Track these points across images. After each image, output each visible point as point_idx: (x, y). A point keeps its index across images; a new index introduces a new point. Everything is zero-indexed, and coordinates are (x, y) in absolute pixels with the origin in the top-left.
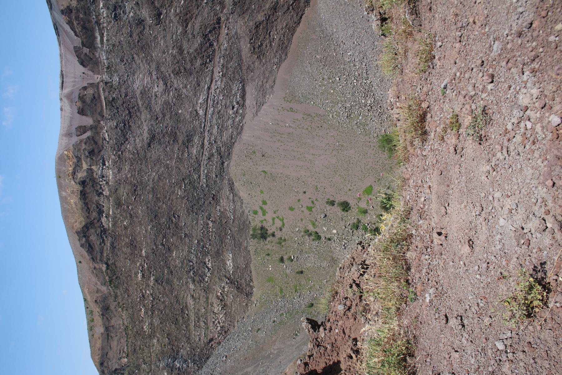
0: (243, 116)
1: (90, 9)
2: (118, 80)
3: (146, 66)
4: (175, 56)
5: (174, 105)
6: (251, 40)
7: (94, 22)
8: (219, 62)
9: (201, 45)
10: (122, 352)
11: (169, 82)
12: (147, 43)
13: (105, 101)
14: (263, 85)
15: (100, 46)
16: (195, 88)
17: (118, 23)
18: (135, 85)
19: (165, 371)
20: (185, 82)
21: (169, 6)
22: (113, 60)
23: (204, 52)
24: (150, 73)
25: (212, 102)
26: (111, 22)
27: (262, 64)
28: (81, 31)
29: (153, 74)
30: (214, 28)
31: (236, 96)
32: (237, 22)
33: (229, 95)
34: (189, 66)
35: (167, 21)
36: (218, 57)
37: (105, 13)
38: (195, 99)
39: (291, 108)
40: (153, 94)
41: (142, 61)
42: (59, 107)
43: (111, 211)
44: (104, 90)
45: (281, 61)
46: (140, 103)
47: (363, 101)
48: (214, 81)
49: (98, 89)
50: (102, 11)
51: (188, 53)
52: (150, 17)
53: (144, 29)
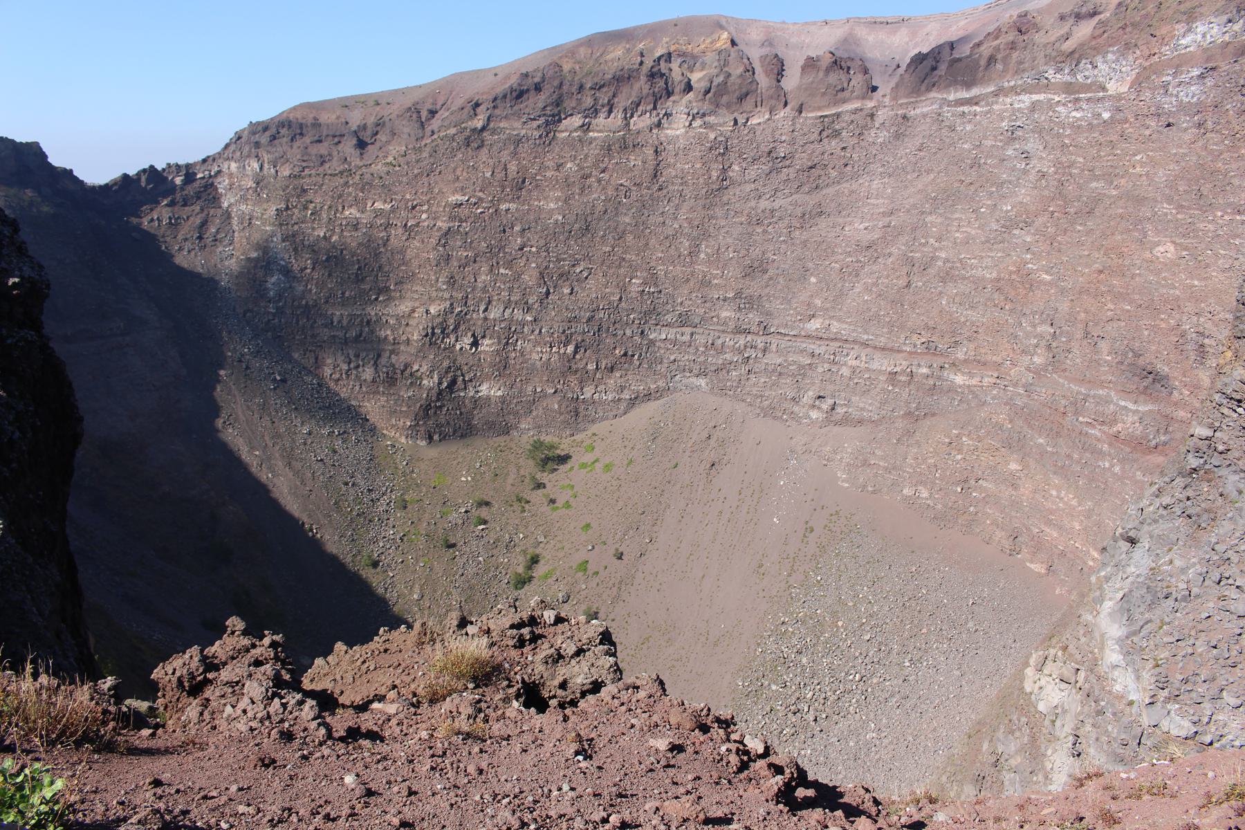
10: (304, 164)
13: (834, 115)
15: (952, 97)
19: (261, 254)
42: (828, 18)
43: (596, 134)
46: (830, 191)
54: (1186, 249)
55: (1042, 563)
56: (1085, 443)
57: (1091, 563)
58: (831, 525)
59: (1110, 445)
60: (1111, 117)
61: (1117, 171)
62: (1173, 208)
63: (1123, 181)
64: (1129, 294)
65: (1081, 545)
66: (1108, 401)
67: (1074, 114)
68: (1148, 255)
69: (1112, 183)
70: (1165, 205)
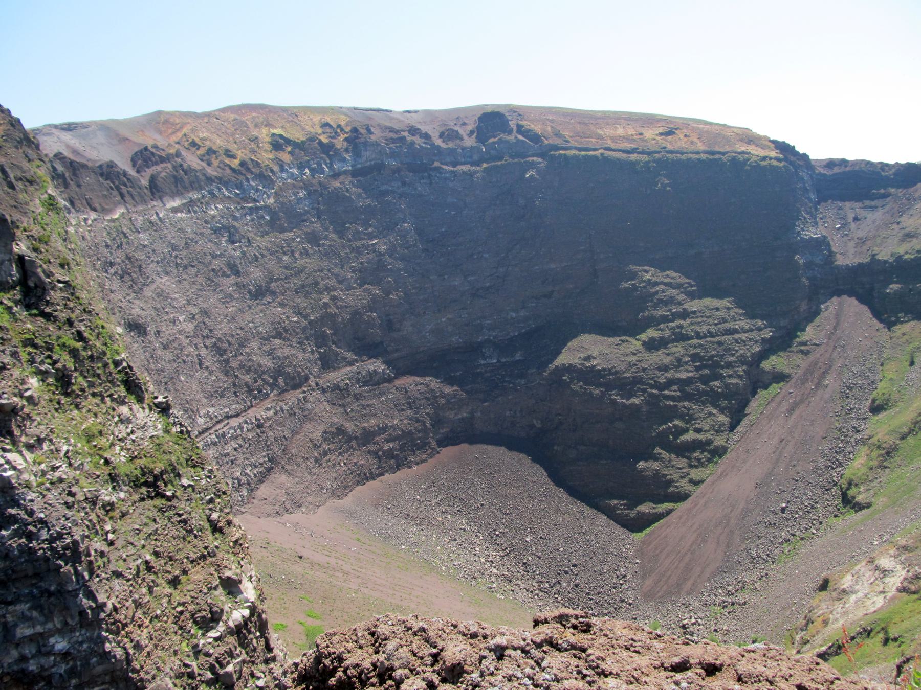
0: (243, 503)
4: (233, 336)
5: (184, 362)
6: (325, 432)
8: (268, 409)
14: (303, 493)
15: (168, 206)
17: (212, 234)
21: (279, 303)
23: (262, 380)
26: (206, 222)
30: (293, 378)
34: (234, 364)
35: (261, 308)
46: (148, 292)
53: (228, 276)
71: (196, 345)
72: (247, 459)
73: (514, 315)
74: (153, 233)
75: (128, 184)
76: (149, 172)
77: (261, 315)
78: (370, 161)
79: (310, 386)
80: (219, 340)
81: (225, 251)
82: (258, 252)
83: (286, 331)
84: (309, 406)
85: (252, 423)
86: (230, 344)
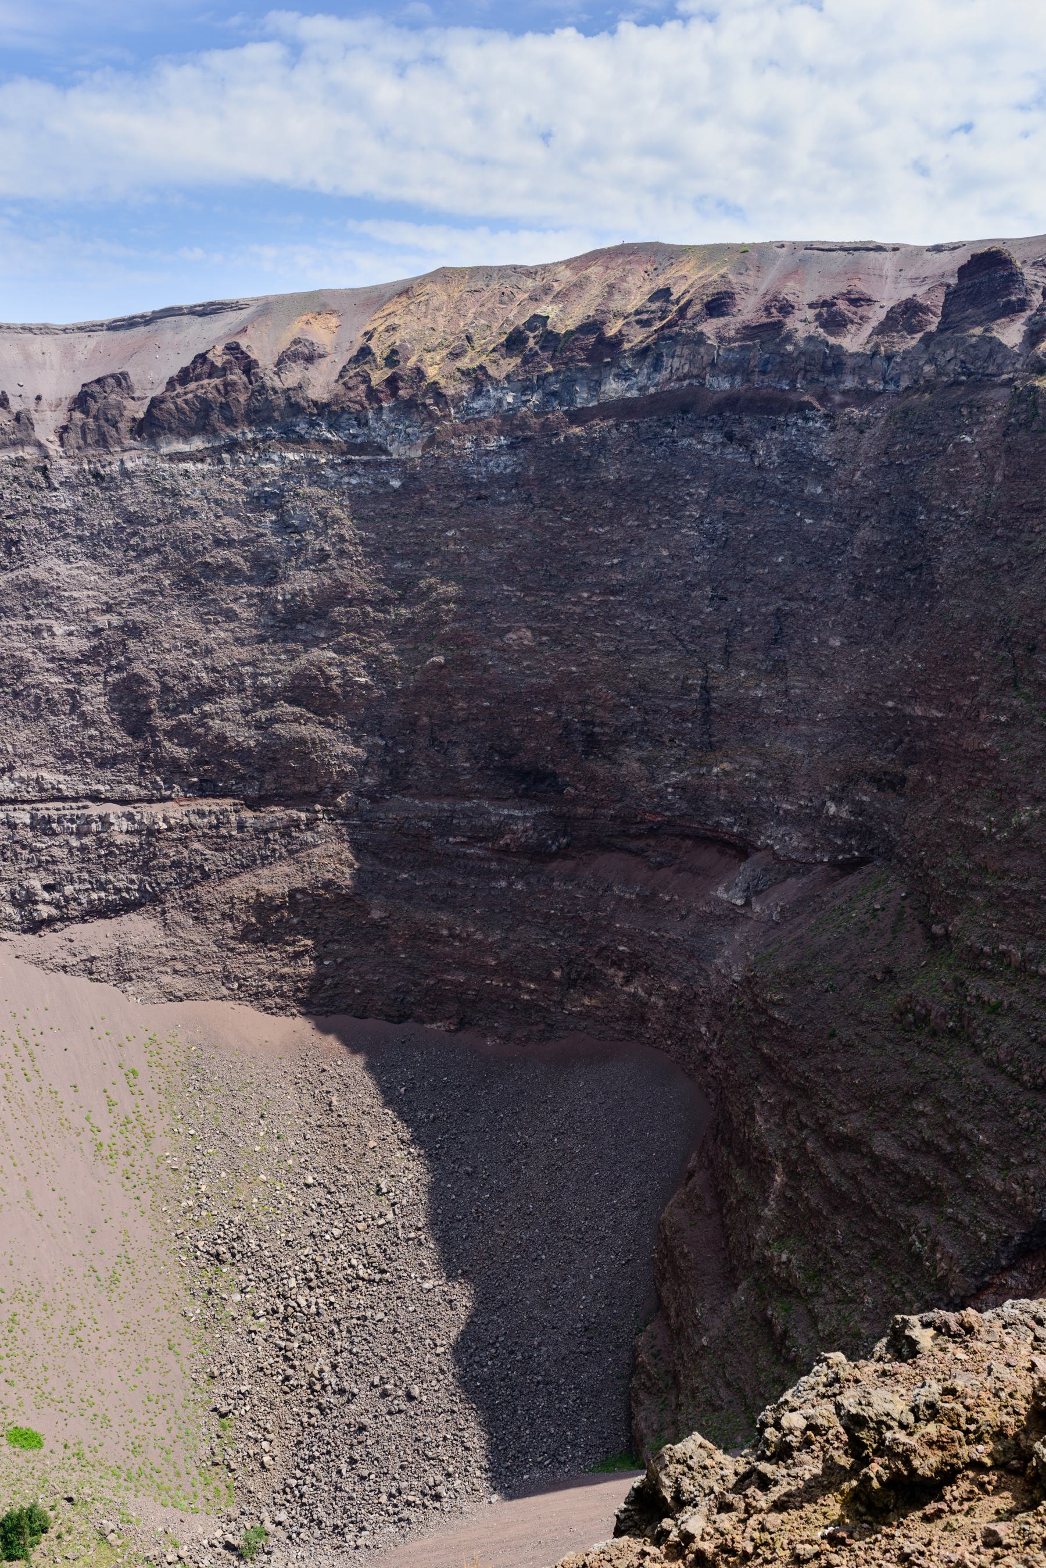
1: (269, 423)
2: (63, 506)
3: (131, 591)
4: (186, 678)
5: (16, 694)
7: (234, 434)
9: (242, 754)
11: (90, 669)
12: (203, 593)
15: (165, 450)
16: (89, 755)
18: (56, 560)
20: (106, 718)
22: (127, 491)
24: (109, 609)
25: (54, 814)
26: (247, 482)
27: (232, 944)
28: (196, 396)
29: (108, 616)
31: (93, 889)
32: (343, 841)
33: (92, 867)
34: (161, 722)
35: (290, 646)
36: (215, 808)
37: (272, 465)
38: (51, 759)
39: (133, 1072)
40: (43, 622)
41: (143, 580)
44: (19, 462)
45: (256, 996)
47: (293, 1283)
48: (128, 809)
49: (14, 444)
50: (275, 458)
51: (205, 715)
52: (294, 595)
53: (250, 580)
54: (546, 634)
55: (448, 1018)
56: (465, 867)
57: (526, 997)
58: (154, 1059)
59: (500, 861)
60: (403, 485)
61: (427, 549)
62: (517, 590)
63: (436, 561)
64: (484, 689)
65: (503, 981)
66: (483, 813)
67: (346, 479)
68: (497, 642)
69: (422, 562)
70: (505, 588)
71: (78, 677)
72: (89, 872)
73: (832, 809)
74: (97, 491)
75: (92, 414)
76: (180, 389)
77: (283, 657)
78: (680, 379)
79: (336, 805)
80: (141, 680)
81: (264, 535)
82: (334, 544)
83: (328, 693)
84: (308, 836)
85: (141, 823)
86: (166, 689)
